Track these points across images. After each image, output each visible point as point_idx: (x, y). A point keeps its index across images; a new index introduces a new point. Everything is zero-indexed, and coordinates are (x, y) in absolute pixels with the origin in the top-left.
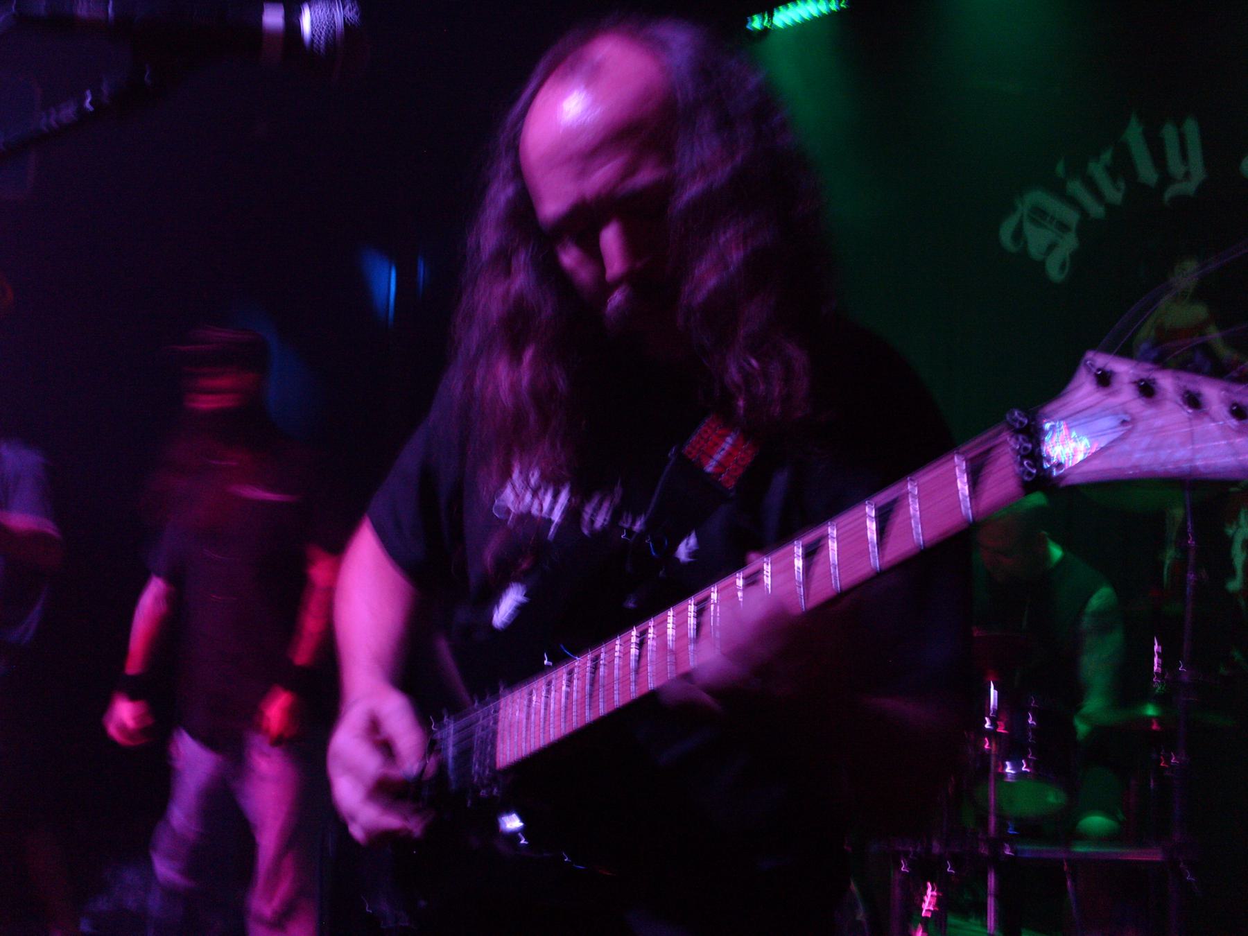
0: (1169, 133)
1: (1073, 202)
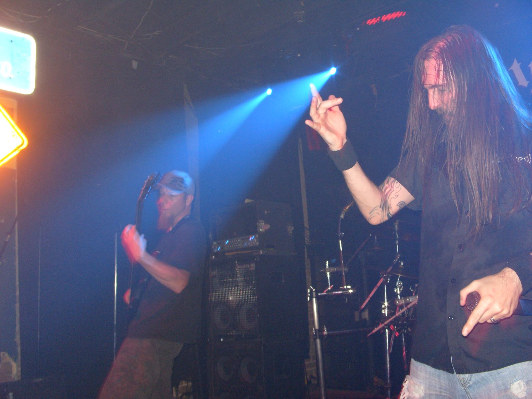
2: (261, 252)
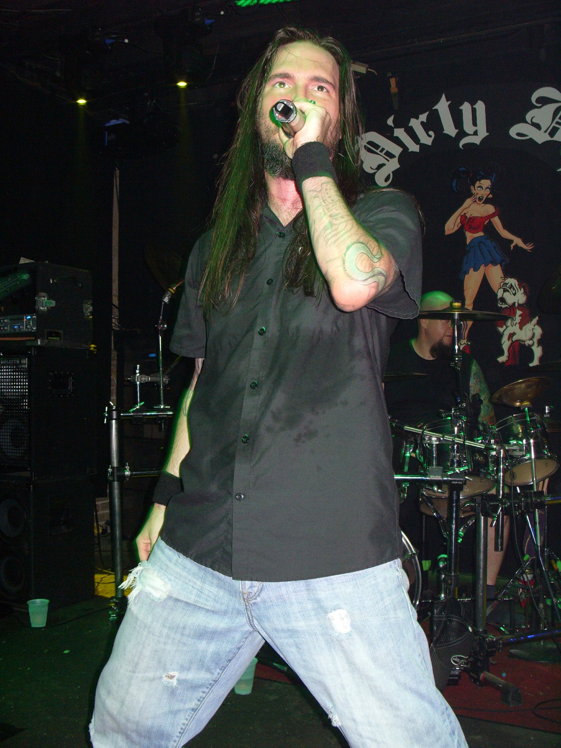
0: (466, 108)
1: (397, 141)
2: (39, 343)
